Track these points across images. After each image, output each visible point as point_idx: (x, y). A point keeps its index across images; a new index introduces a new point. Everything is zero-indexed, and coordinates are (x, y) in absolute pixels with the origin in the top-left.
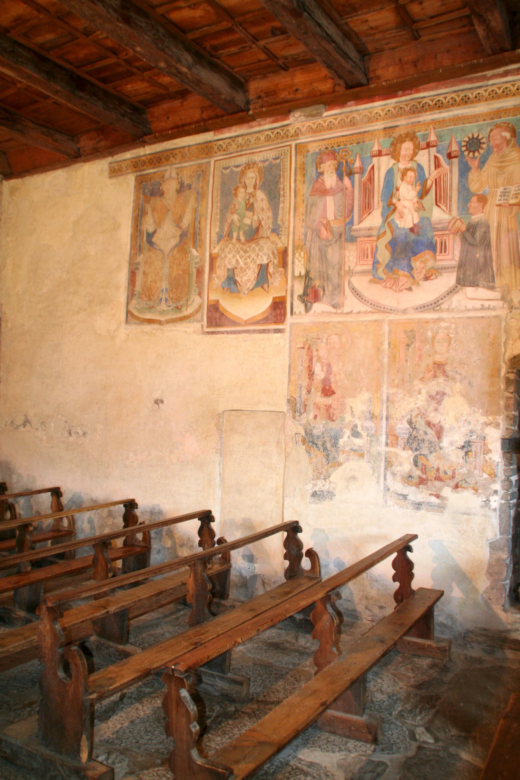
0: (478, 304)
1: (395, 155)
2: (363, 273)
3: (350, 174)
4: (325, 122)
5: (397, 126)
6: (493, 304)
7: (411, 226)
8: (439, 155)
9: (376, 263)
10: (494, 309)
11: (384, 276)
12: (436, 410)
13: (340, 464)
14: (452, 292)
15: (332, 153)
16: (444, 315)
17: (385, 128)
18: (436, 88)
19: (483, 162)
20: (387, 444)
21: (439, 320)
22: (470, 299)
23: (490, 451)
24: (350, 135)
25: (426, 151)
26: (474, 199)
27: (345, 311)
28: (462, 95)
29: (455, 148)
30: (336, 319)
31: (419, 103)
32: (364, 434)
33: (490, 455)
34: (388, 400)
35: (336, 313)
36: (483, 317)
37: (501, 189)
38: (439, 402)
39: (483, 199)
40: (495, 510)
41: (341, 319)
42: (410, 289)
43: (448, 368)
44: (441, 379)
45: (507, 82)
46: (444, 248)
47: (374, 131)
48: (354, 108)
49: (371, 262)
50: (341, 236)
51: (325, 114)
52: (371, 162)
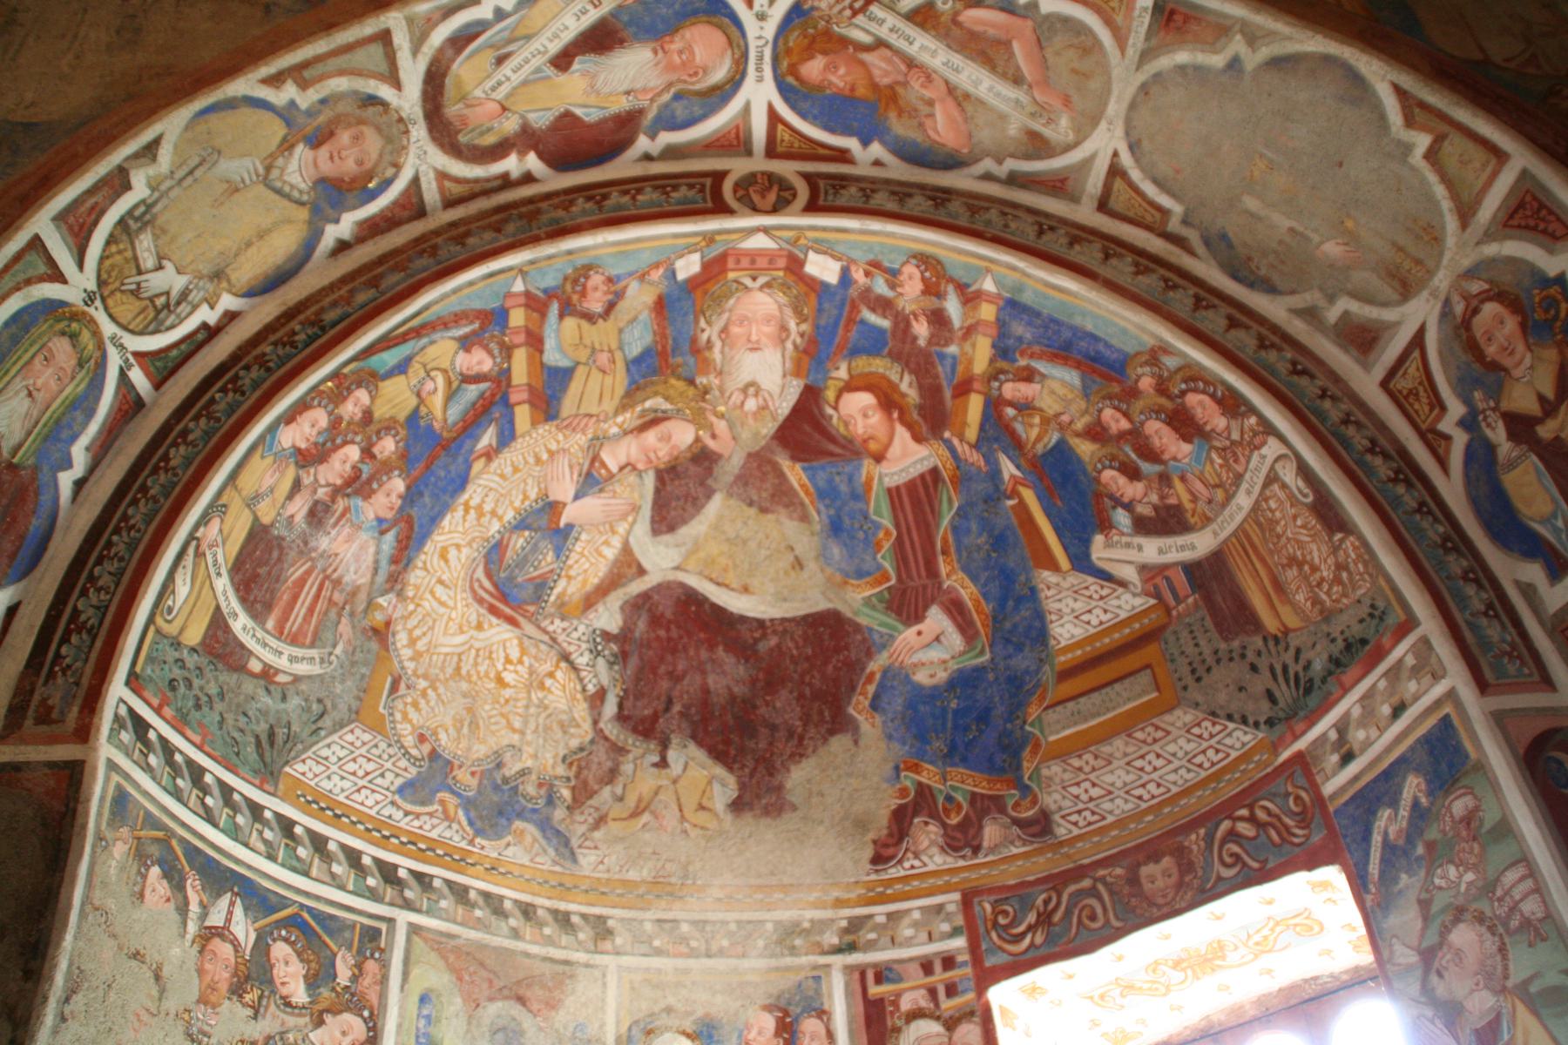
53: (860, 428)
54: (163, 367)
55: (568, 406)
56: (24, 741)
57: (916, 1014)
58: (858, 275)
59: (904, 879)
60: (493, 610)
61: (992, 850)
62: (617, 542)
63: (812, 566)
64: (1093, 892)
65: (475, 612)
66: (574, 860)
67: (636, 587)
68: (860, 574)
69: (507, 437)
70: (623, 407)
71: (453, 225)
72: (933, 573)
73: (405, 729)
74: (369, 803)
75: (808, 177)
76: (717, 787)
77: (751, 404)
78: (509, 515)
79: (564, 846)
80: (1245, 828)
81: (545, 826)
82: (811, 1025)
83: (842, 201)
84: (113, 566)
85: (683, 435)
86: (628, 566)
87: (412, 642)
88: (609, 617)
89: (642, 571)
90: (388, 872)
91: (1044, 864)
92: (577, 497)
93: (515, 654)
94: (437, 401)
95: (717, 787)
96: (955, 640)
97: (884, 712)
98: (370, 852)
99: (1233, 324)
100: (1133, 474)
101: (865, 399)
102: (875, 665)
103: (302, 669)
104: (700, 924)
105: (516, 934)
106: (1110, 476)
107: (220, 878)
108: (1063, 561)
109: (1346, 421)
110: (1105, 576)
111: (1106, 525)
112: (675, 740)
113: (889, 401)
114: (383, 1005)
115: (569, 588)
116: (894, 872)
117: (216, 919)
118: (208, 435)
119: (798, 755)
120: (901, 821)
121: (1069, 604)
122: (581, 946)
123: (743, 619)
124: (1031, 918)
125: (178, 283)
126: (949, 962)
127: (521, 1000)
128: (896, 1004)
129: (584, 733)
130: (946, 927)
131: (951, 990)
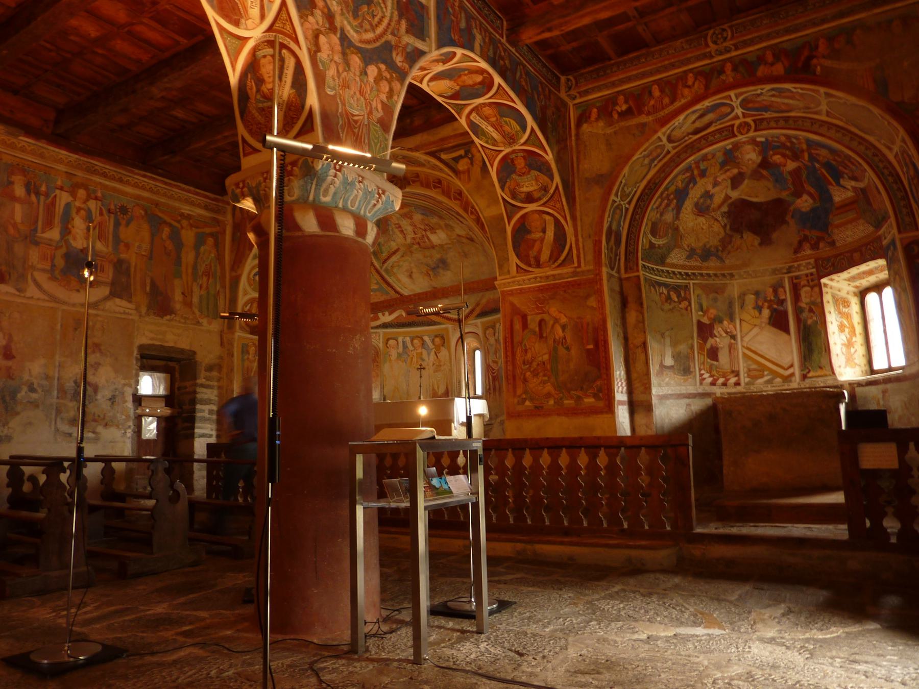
0: (122, 310)
1: (73, 194)
2: (44, 270)
3: (37, 194)
4: (19, 143)
5: (75, 175)
6: (130, 311)
7: (81, 248)
8: (103, 208)
9: (53, 266)
10: (131, 315)
11: (58, 276)
12: (94, 374)
13: (17, 414)
14: (106, 299)
15: (24, 172)
16: (100, 313)
17: (66, 172)
18: (105, 163)
19: (127, 225)
20: (58, 398)
21: (97, 315)
22: (118, 306)
23: (126, 402)
24: (39, 164)
25: (94, 201)
26: (122, 244)
27: (27, 296)
28: (120, 176)
29: (112, 207)
30: (19, 300)
31: (93, 167)
32: (40, 390)
33: (127, 404)
34: (59, 365)
35: (19, 296)
36: (124, 319)
37: (137, 244)
38: (96, 370)
39: (127, 246)
40: (129, 438)
41: (24, 301)
42: (78, 291)
43: (102, 348)
44: (98, 355)
45: (145, 182)
46: (102, 270)
47: (57, 170)
48: (45, 146)
49: (50, 264)
50: (26, 238)
51: (21, 138)
52: (54, 192)
53: (778, 161)
54: (629, 203)
55: (707, 174)
58: (770, 139)
60: (698, 215)
62: (724, 194)
64: (844, 259)
65: (694, 217)
66: (724, 262)
67: (730, 201)
69: (695, 183)
71: (676, 153)
74: (681, 262)
75: (754, 121)
77: (750, 162)
78: (698, 196)
79: (721, 259)
80: (872, 248)
82: (781, 290)
83: (762, 127)
84: (633, 241)
85: (735, 171)
86: (727, 197)
87: (683, 227)
88: (725, 209)
89: (731, 198)
90: (687, 274)
92: (713, 188)
93: (704, 222)
96: (811, 201)
98: (683, 271)
99: (860, 143)
100: (846, 169)
101: (778, 156)
102: (792, 208)
103: (664, 242)
105: (714, 280)
106: (840, 168)
107: (660, 284)
108: (834, 183)
110: (845, 188)
111: (843, 177)
113: (784, 156)
114: (691, 299)
115: (714, 205)
116: (799, 255)
117: (661, 291)
120: (800, 243)
125: (630, 189)
126: (812, 274)
127: (717, 293)
129: (723, 234)
130: (811, 267)
131: (812, 280)
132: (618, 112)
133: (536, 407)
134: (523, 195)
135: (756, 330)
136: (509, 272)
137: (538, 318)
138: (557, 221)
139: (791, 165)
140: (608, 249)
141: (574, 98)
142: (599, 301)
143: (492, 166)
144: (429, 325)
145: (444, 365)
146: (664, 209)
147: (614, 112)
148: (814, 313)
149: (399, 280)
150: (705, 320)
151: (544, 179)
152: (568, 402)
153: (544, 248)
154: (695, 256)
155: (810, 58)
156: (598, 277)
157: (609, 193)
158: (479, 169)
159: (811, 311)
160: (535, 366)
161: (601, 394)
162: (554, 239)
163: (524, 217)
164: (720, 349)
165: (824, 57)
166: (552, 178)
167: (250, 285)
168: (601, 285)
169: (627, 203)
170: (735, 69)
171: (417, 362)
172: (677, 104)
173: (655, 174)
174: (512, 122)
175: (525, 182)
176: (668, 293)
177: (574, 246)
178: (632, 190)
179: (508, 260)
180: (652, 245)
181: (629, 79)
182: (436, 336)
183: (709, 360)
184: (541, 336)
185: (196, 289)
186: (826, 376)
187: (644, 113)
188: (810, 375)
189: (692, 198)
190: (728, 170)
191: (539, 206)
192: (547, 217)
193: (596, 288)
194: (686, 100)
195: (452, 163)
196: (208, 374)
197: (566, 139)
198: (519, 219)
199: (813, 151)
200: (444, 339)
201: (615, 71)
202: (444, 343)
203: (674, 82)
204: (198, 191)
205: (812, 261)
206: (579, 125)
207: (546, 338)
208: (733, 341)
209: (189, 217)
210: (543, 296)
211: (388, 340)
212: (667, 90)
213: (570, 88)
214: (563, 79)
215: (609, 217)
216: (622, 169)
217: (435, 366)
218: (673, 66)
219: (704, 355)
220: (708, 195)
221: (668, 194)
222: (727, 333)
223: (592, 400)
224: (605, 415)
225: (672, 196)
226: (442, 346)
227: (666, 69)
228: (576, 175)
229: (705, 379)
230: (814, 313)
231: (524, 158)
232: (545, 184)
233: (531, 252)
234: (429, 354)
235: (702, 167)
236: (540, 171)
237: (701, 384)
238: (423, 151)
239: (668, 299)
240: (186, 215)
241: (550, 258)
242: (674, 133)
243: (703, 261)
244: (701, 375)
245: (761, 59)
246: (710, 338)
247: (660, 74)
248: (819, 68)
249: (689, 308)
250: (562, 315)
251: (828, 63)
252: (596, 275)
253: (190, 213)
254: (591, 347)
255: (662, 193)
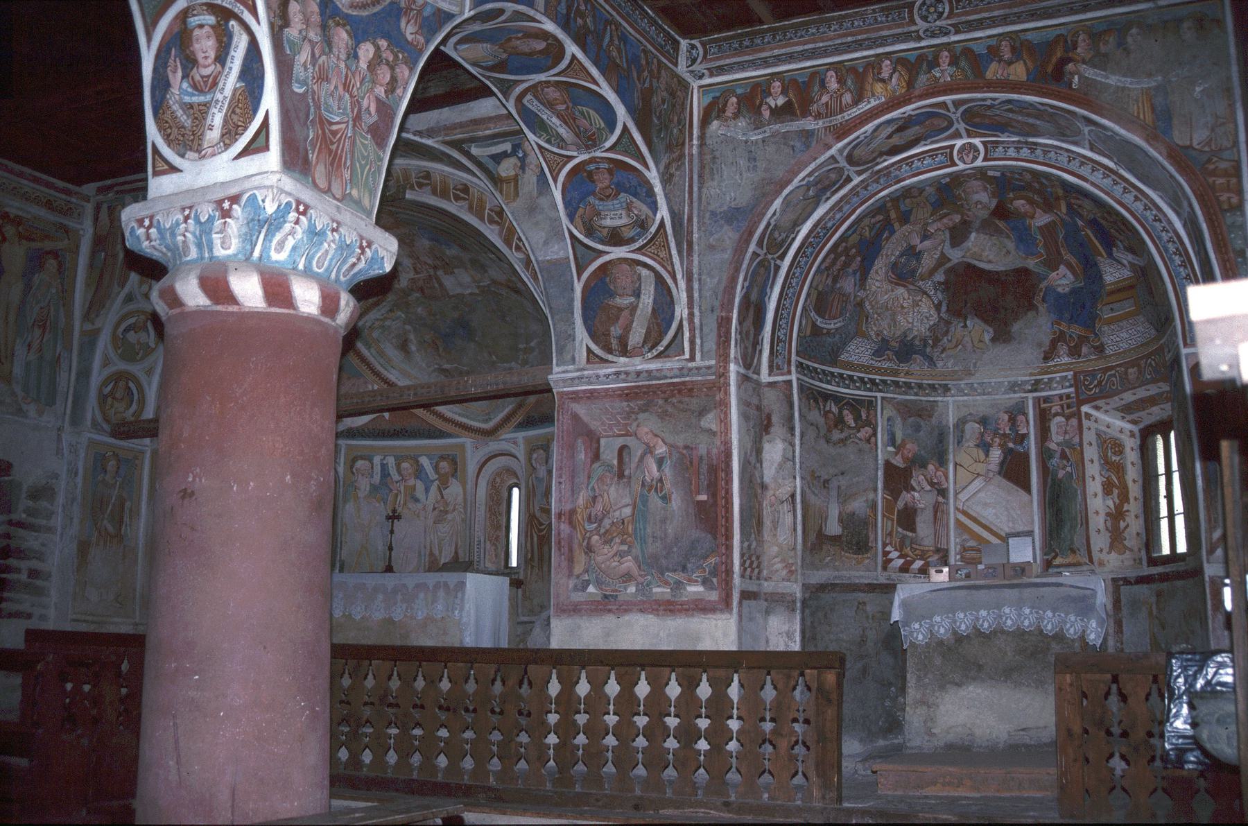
55: (912, 219)
56: (775, 375)
57: (1057, 414)
59: (1055, 366)
61: (1085, 357)
63: (1013, 252)
67: (948, 265)
68: (1032, 254)
69: (893, 232)
70: (932, 215)
71: (862, 181)
72: (1060, 253)
73: (872, 333)
74: (864, 361)
75: (984, 143)
76: (985, 333)
79: (931, 361)
81: (924, 355)
82: (1021, 418)
83: (996, 156)
85: (957, 218)
86: (944, 259)
87: (870, 303)
88: (940, 277)
89: (949, 260)
90: (872, 381)
91: (1101, 364)
93: (906, 297)
94: (867, 233)
95: (985, 333)
97: (1046, 302)
98: (866, 376)
99: (1136, 198)
101: (1022, 202)
102: (1043, 285)
104: (981, 384)
105: (916, 394)
107: (827, 396)
108: (1104, 253)
109: (1169, 241)
111: (1116, 246)
112: (969, 317)
113: (1031, 202)
116: (1051, 363)
117: (827, 408)
118: (801, 273)
119: (1016, 319)
120: (1054, 343)
121: (1108, 269)
122: (939, 395)
123: (990, 272)
124: (1096, 382)
125: (784, 235)
126: (1068, 396)
127: (920, 416)
128: (1050, 410)
130: (1067, 384)
131: (1069, 407)
132: (770, 107)
133: (606, 597)
134: (605, 232)
135: (978, 483)
136: (573, 360)
137: (620, 441)
138: (659, 280)
139: (1042, 219)
140: (740, 333)
141: (701, 77)
142: (721, 421)
143: (555, 181)
144: (430, 436)
145: (454, 510)
146: (839, 270)
147: (764, 107)
148: (1068, 460)
149: (381, 354)
150: (898, 461)
151: (641, 208)
152: (660, 591)
153: (635, 324)
154: (888, 352)
155: (1064, 61)
156: (722, 380)
157: (748, 242)
158: (535, 179)
159: (1064, 456)
160: (608, 527)
161: (715, 580)
162: (653, 309)
163: (603, 267)
164: (919, 511)
165: (1084, 62)
166: (654, 207)
167: (116, 348)
168: (727, 393)
169: (778, 258)
170: (954, 62)
171: (405, 504)
172: (864, 107)
173: (827, 213)
174: (592, 112)
175: (610, 210)
176: (840, 412)
177: (685, 324)
178: (787, 237)
179: (574, 340)
180: (816, 330)
181: (790, 58)
182: (442, 458)
183: (900, 530)
184: (621, 475)
185: (20, 351)
186: (1080, 564)
187: (811, 115)
188: (1058, 561)
189: (887, 255)
190: (945, 215)
191: (633, 251)
192: (644, 272)
193: (717, 398)
194: (878, 102)
195: (491, 165)
196: (30, 503)
197: (683, 144)
198: (595, 271)
199: (1073, 201)
200: (456, 463)
201: (769, 43)
202: (456, 470)
203: (861, 70)
204: (38, 174)
205: (1070, 374)
206: (705, 122)
207: (630, 477)
208: (941, 499)
209: (18, 221)
210: (628, 406)
211: (354, 460)
212: (849, 82)
213: (694, 61)
214: (684, 44)
215: (745, 280)
216: (772, 202)
217: (436, 512)
218: (859, 45)
219: (893, 520)
220: (912, 253)
221: (846, 247)
222: (932, 484)
223: (701, 589)
224: (718, 616)
225: (854, 250)
226: (453, 476)
227: (848, 48)
228: (695, 205)
229: (891, 560)
230: (1068, 460)
231: (610, 171)
232: (643, 217)
233: (612, 329)
234: (427, 490)
235: (902, 208)
236: (635, 195)
237: (885, 568)
238: (440, 139)
239: (840, 422)
240: (12, 216)
241: (645, 342)
242: (857, 152)
243: (901, 362)
244: (886, 554)
245: (993, 52)
246: (904, 492)
247: (840, 54)
248: (1076, 77)
249: (873, 439)
250: (660, 442)
251: (1090, 73)
252: (720, 377)
253: (20, 213)
254: (704, 497)
255: (836, 245)
